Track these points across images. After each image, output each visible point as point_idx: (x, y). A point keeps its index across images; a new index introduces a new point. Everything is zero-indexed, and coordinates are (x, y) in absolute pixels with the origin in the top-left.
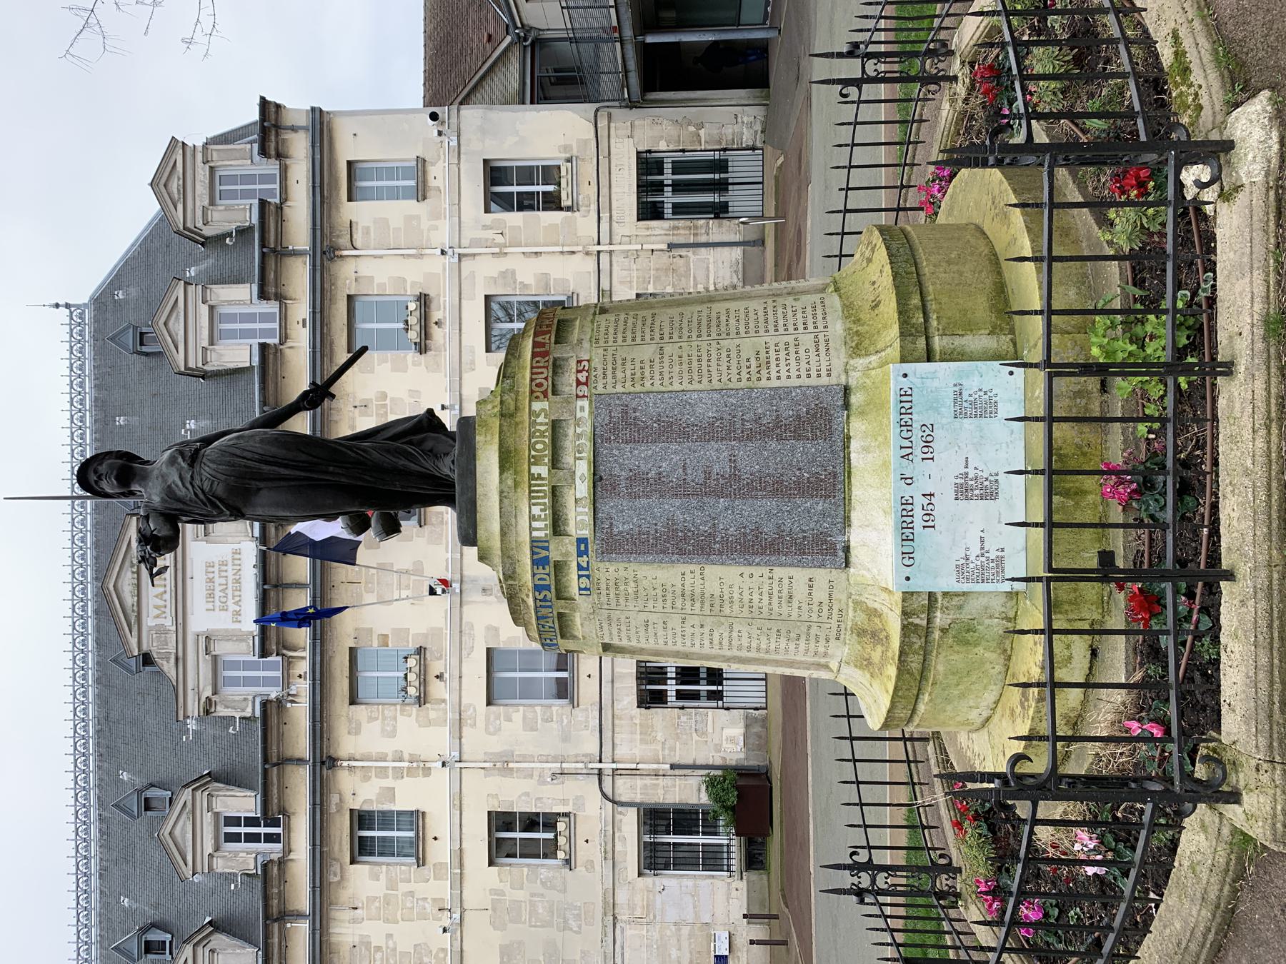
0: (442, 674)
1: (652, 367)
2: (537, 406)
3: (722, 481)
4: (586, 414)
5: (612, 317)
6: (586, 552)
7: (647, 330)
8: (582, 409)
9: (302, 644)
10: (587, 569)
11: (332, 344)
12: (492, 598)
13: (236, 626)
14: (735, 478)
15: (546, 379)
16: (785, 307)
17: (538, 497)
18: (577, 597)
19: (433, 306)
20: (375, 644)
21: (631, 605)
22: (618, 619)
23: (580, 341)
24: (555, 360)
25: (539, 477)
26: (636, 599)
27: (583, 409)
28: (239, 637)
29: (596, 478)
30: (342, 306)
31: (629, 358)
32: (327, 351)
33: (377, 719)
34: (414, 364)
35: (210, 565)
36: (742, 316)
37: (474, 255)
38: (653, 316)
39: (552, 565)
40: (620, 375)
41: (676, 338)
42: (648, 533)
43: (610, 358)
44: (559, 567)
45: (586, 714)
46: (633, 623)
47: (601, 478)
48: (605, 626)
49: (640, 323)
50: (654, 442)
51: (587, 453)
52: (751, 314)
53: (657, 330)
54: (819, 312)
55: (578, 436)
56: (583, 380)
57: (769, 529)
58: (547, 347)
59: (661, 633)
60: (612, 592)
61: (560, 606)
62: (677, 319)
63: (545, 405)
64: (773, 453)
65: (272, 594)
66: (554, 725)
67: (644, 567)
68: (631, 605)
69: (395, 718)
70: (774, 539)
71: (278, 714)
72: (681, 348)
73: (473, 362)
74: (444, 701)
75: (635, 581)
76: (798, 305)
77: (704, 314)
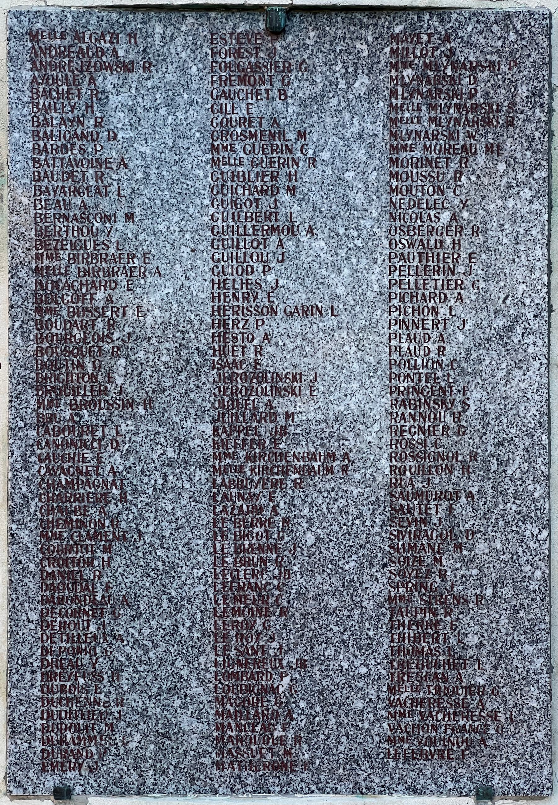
3: (266, 429)
14: (278, 469)
47: (276, 32)
57: (120, 572)
64: (352, 587)
70: (89, 587)
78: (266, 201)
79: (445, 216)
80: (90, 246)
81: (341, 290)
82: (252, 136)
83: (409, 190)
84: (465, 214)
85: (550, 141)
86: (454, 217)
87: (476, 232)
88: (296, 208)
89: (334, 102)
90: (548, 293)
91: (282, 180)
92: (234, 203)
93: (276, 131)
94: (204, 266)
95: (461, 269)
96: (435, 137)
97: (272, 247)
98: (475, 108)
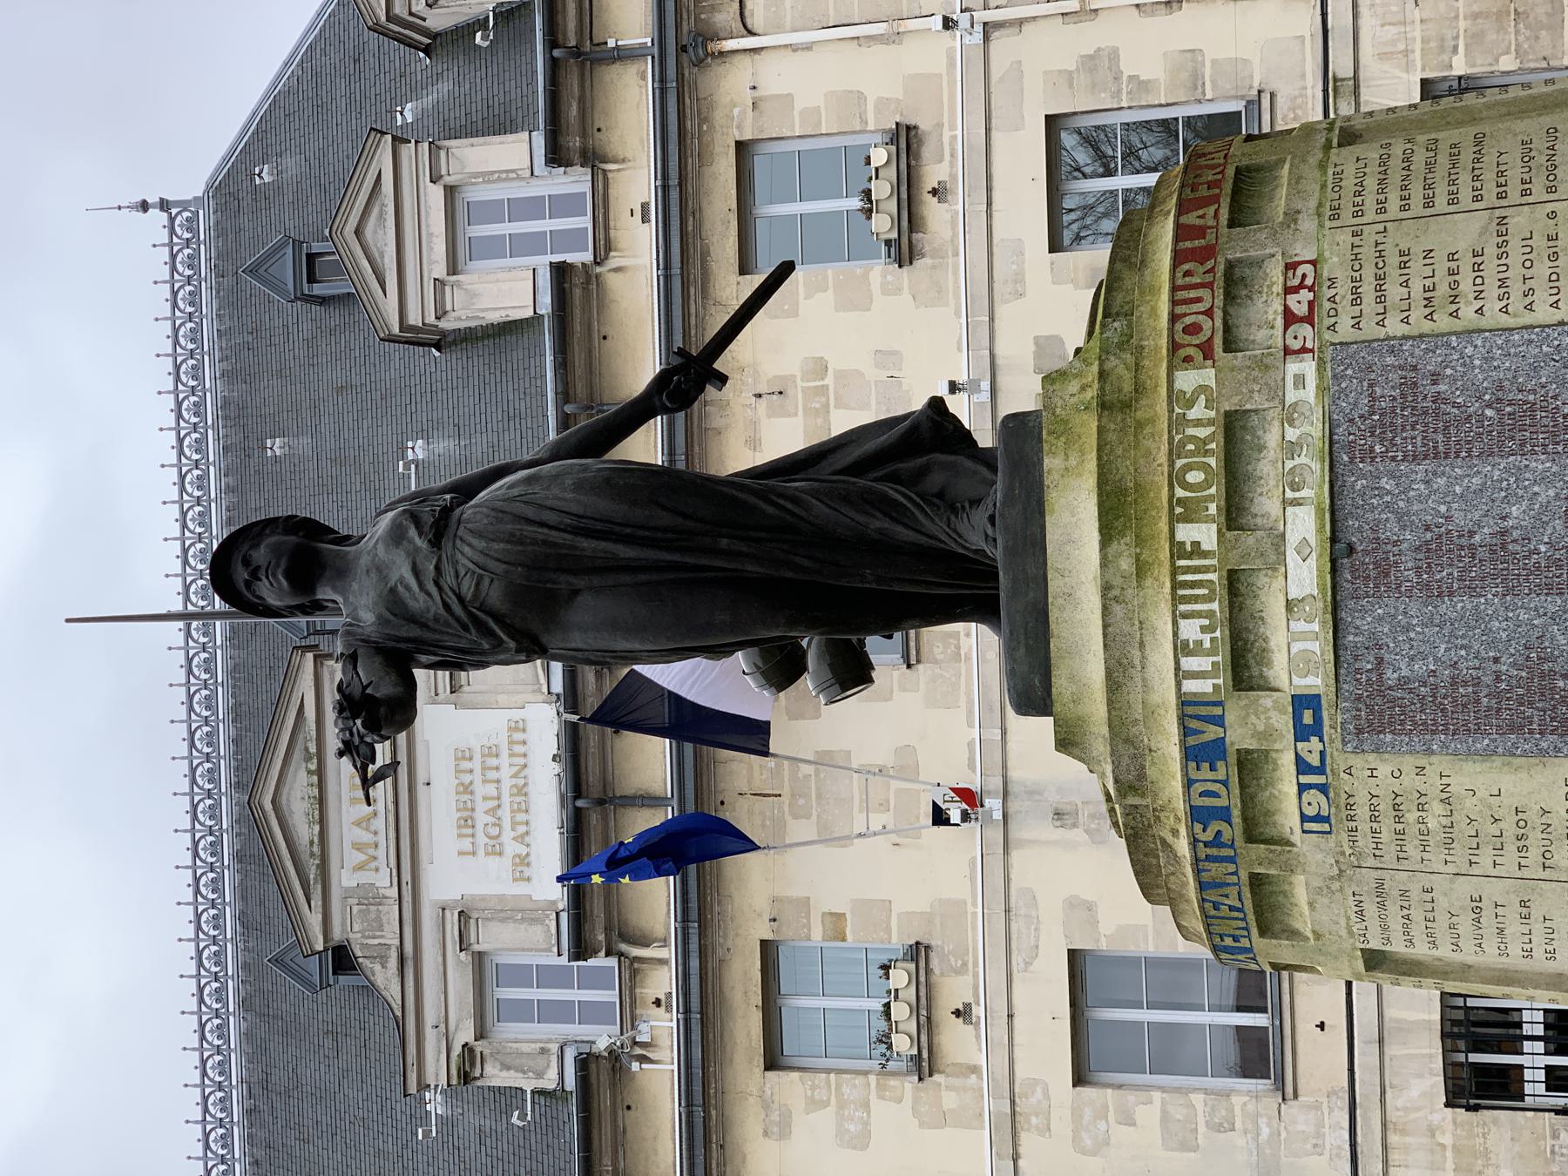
0: (968, 1006)
1: (1477, 268)
2: (1187, 380)
4: (1310, 393)
5: (1371, 152)
6: (1316, 730)
7: (1465, 179)
8: (1300, 381)
9: (659, 931)
10: (1320, 770)
11: (705, 254)
12: (1078, 834)
13: (520, 889)
15: (1209, 313)
17: (1196, 599)
18: (1297, 837)
19: (927, 152)
20: (817, 934)
21: (1436, 859)
22: (1404, 893)
23: (1292, 216)
24: (1231, 266)
25: (1196, 550)
26: (1449, 844)
27: (1303, 381)
28: (525, 913)
29: (1339, 550)
30: (724, 169)
31: (1418, 250)
32: (696, 271)
33: (826, 1104)
34: (885, 291)
35: (463, 755)
37: (1020, 22)
38: (1479, 141)
39: (1232, 759)
40: (1394, 292)
41: (1539, 193)
42: (1477, 682)
43: (1368, 253)
44: (1251, 766)
45: (1316, 1119)
46: (1442, 903)
47: (1351, 549)
48: (1371, 909)
49: (1443, 160)
50: (1486, 454)
51: (1315, 489)
53: (1489, 176)
55: (1291, 449)
56: (1301, 310)
58: (1211, 236)
59: (1514, 928)
60: (1387, 827)
61: (1254, 858)
62: (1540, 143)
63: (1207, 376)
65: (594, 818)
66: (1239, 1140)
67: (1469, 766)
68: (1436, 859)
69: (866, 1106)
71: (614, 1085)
72: (1553, 215)
73: (1019, 278)
74: (975, 1069)
75: (1446, 801)
78: (1482, 553)
79: (1489, 412)
80: (1521, 691)
81: (1551, 493)
82: (1429, 566)
83: (1469, 443)
84: (1487, 397)
85: (1427, 335)
86: (1489, 406)
87: (1501, 388)
88: (1486, 530)
89: (1401, 504)
90: (1548, 326)
91: (1464, 541)
92: (1483, 579)
93: (1423, 548)
94: (1536, 601)
95: (1531, 397)
96: (1426, 425)
97: (1518, 548)
98: (1403, 396)
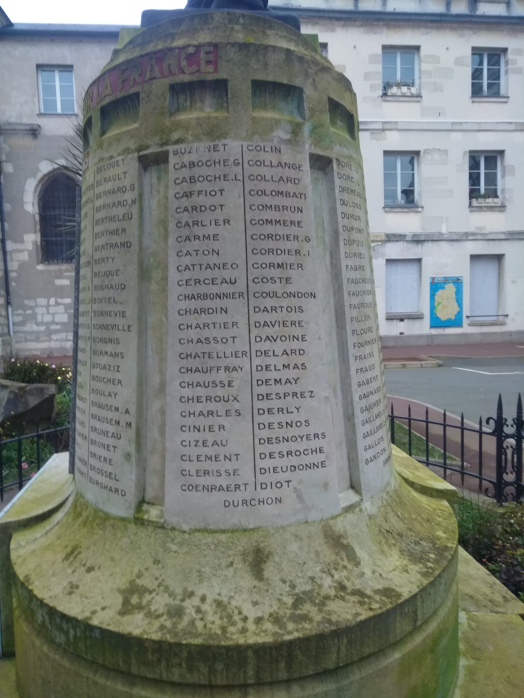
16: (117, 436)
36: (110, 375)
52: (110, 388)
54: (103, 480)
76: (117, 457)
77: (120, 321)
